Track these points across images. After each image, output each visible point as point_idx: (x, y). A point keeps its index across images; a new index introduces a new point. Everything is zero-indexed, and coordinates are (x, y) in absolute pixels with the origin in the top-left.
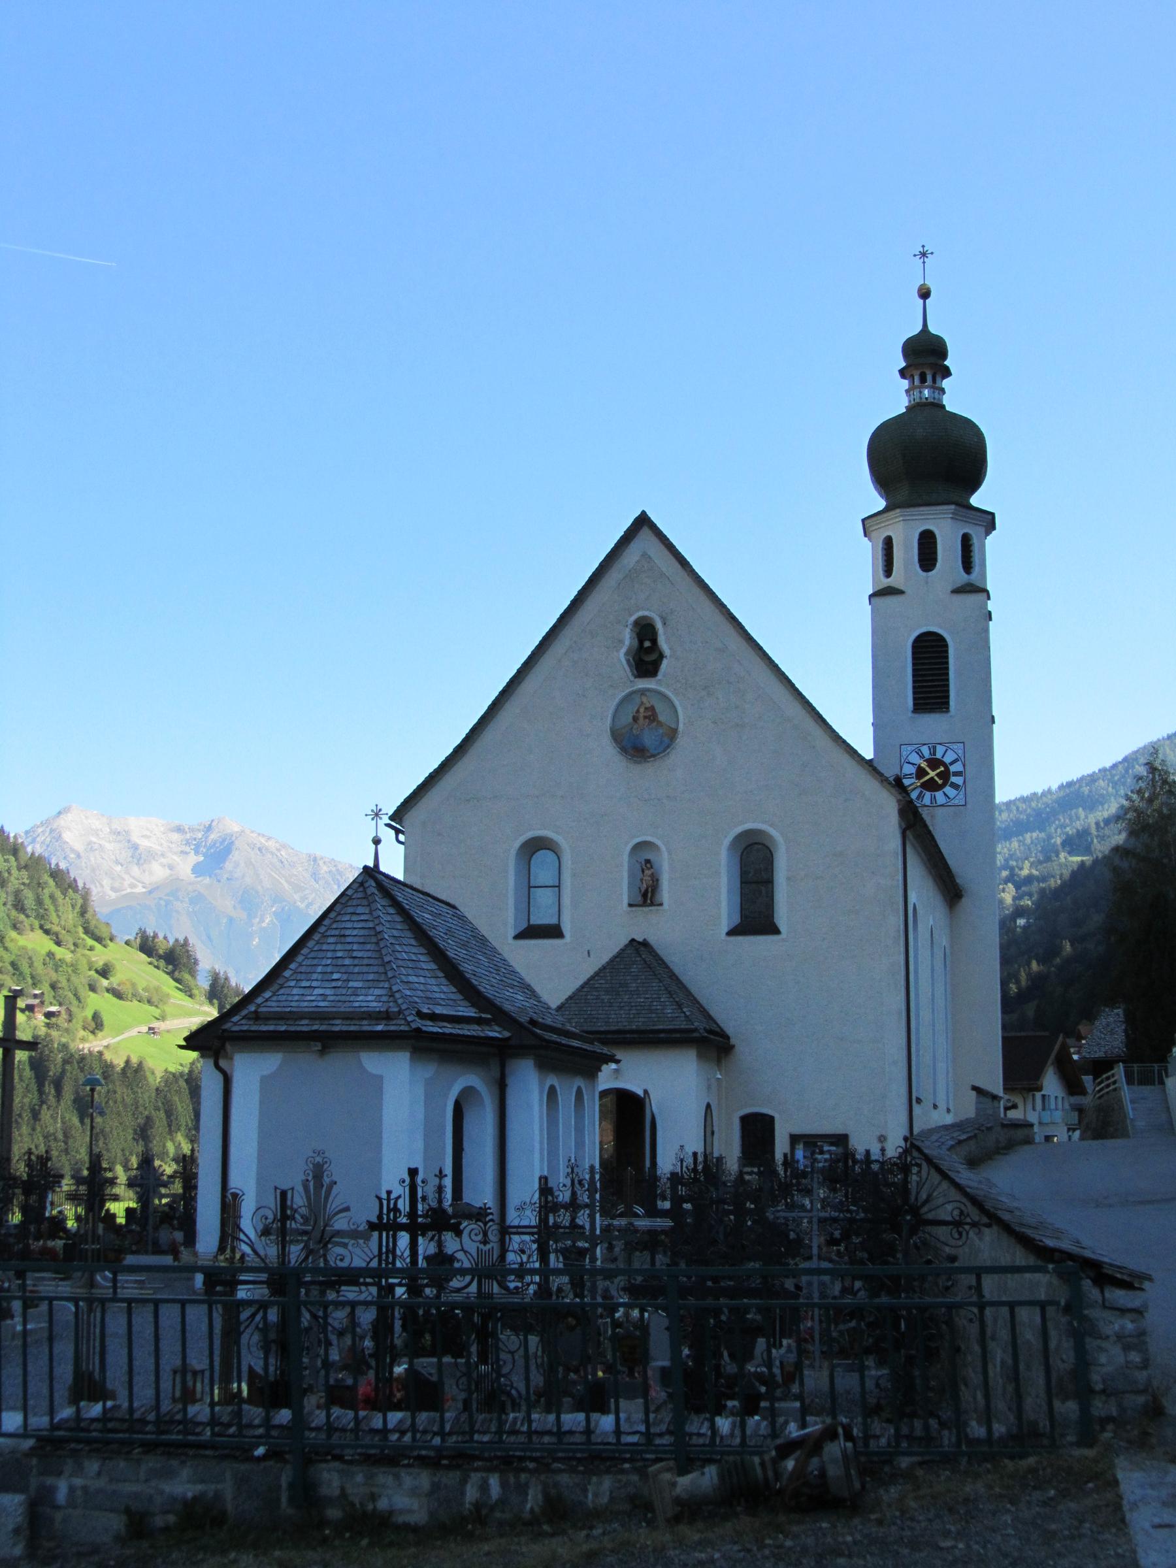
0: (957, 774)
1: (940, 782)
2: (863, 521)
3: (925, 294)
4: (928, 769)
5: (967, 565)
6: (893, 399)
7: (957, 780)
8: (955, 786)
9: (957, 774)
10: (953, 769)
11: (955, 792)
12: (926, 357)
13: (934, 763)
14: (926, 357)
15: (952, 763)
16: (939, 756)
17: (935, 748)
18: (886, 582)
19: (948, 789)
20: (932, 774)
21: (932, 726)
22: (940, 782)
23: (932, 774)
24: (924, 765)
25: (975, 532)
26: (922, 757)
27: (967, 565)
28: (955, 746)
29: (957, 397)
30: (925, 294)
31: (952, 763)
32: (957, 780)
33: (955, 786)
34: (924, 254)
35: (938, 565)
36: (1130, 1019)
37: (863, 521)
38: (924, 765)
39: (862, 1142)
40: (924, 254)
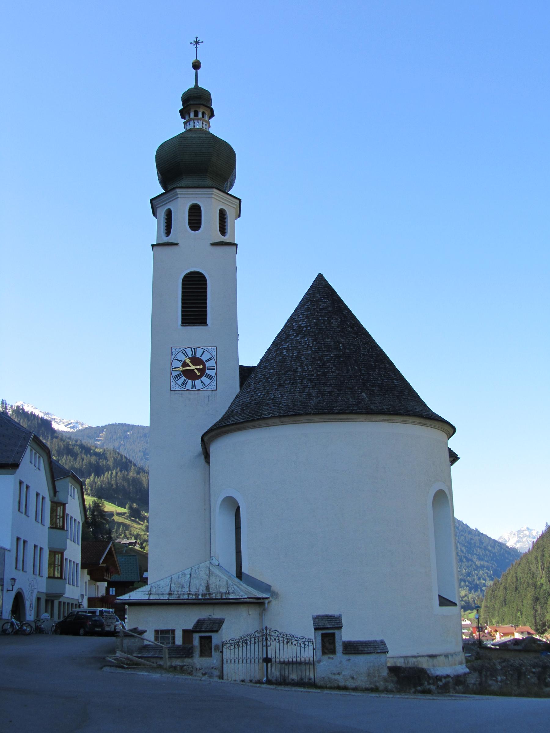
0: (210, 368)
1: (198, 374)
2: (152, 200)
3: (196, 66)
4: (190, 364)
5: (223, 230)
6: (176, 127)
7: (211, 373)
8: (210, 377)
9: (210, 368)
10: (208, 364)
11: (209, 381)
12: (196, 103)
13: (196, 361)
14: (196, 103)
15: (207, 361)
16: (198, 355)
17: (195, 350)
18: (165, 239)
19: (204, 379)
20: (193, 367)
21: (195, 333)
22: (198, 374)
23: (193, 367)
24: (188, 361)
25: (230, 214)
26: (186, 356)
27: (223, 230)
28: (210, 349)
29: (218, 128)
30: (196, 66)
31: (207, 361)
32: (211, 373)
33: (210, 377)
34: (197, 43)
35: (202, 226)
36: (180, 646)
37: (152, 200)
38: (188, 361)
39: (272, 588)
40: (197, 43)
